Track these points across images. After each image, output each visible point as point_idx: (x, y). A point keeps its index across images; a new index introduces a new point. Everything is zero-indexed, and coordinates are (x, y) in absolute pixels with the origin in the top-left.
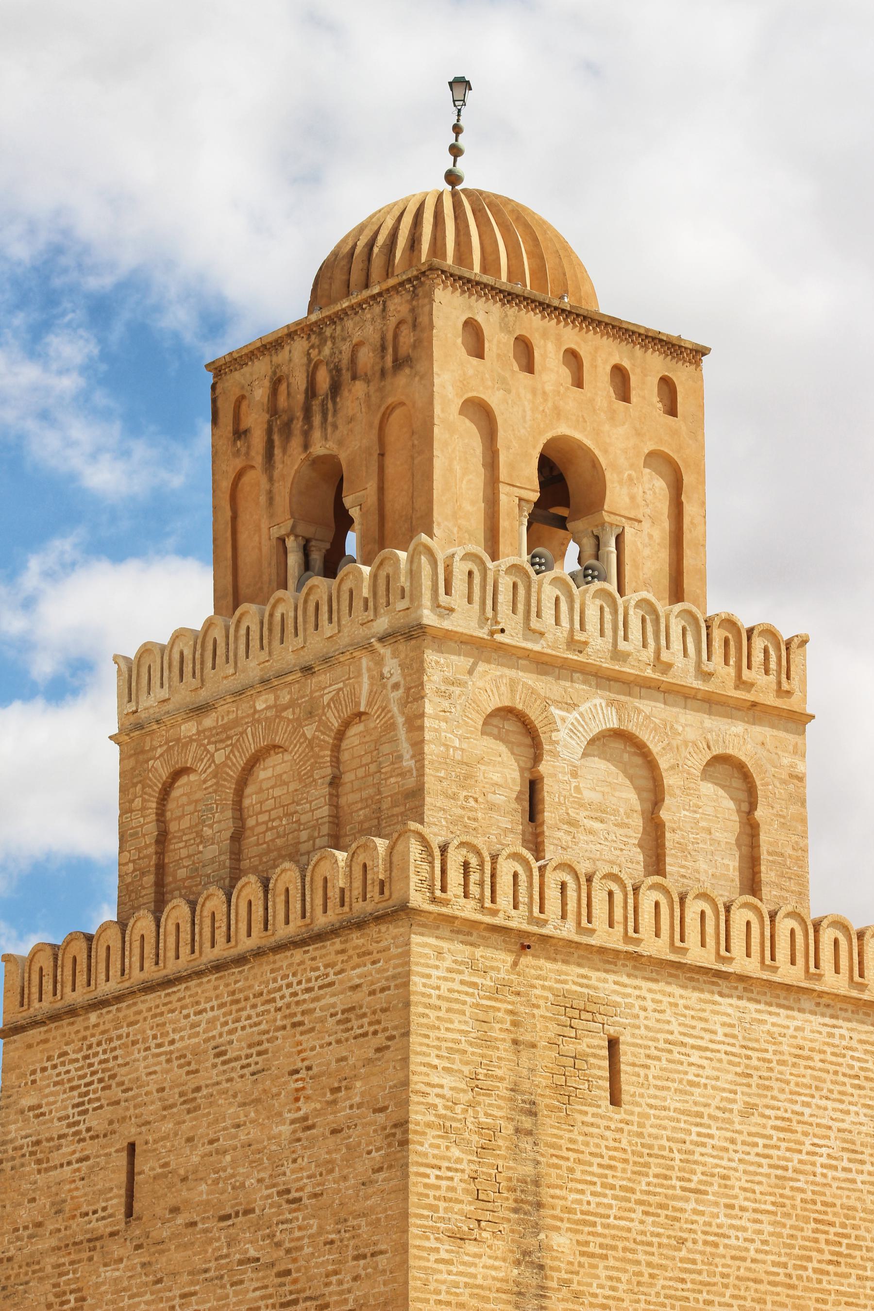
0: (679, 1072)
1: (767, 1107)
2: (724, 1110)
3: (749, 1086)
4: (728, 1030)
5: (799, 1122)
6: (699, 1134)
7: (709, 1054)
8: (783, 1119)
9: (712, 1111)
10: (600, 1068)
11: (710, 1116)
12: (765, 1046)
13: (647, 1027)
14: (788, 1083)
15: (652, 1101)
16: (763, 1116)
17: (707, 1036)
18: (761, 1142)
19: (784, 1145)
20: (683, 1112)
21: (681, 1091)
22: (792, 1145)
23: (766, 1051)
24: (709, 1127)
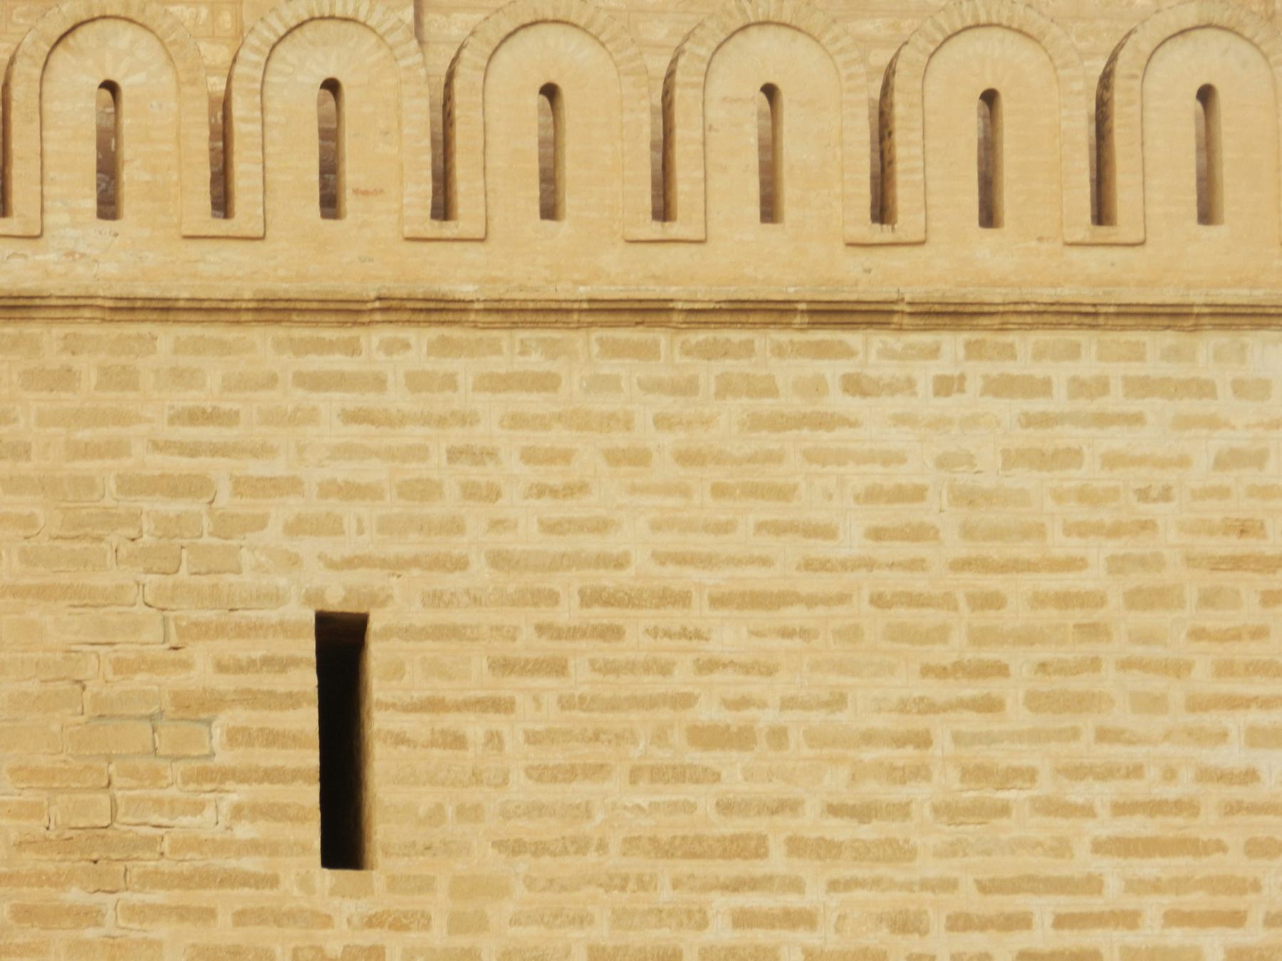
0: (650, 703)
1: (1076, 772)
2: (863, 813)
3: (990, 705)
4: (887, 514)
5: (1233, 808)
6: (743, 919)
7: (794, 615)
8: (1155, 808)
9: (811, 822)
10: (273, 738)
11: (796, 846)
12: (1061, 545)
13: (499, 560)
14: (1179, 669)
15: (523, 828)
16: (1052, 808)
17: (790, 549)
18: (1043, 907)
19: (1153, 906)
20: (663, 849)
21: (659, 774)
22: (1196, 900)
23: (1073, 564)
24: (795, 885)
